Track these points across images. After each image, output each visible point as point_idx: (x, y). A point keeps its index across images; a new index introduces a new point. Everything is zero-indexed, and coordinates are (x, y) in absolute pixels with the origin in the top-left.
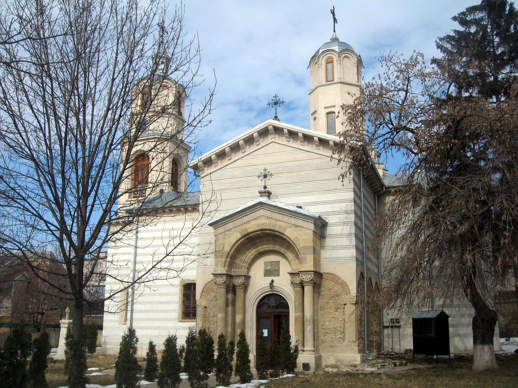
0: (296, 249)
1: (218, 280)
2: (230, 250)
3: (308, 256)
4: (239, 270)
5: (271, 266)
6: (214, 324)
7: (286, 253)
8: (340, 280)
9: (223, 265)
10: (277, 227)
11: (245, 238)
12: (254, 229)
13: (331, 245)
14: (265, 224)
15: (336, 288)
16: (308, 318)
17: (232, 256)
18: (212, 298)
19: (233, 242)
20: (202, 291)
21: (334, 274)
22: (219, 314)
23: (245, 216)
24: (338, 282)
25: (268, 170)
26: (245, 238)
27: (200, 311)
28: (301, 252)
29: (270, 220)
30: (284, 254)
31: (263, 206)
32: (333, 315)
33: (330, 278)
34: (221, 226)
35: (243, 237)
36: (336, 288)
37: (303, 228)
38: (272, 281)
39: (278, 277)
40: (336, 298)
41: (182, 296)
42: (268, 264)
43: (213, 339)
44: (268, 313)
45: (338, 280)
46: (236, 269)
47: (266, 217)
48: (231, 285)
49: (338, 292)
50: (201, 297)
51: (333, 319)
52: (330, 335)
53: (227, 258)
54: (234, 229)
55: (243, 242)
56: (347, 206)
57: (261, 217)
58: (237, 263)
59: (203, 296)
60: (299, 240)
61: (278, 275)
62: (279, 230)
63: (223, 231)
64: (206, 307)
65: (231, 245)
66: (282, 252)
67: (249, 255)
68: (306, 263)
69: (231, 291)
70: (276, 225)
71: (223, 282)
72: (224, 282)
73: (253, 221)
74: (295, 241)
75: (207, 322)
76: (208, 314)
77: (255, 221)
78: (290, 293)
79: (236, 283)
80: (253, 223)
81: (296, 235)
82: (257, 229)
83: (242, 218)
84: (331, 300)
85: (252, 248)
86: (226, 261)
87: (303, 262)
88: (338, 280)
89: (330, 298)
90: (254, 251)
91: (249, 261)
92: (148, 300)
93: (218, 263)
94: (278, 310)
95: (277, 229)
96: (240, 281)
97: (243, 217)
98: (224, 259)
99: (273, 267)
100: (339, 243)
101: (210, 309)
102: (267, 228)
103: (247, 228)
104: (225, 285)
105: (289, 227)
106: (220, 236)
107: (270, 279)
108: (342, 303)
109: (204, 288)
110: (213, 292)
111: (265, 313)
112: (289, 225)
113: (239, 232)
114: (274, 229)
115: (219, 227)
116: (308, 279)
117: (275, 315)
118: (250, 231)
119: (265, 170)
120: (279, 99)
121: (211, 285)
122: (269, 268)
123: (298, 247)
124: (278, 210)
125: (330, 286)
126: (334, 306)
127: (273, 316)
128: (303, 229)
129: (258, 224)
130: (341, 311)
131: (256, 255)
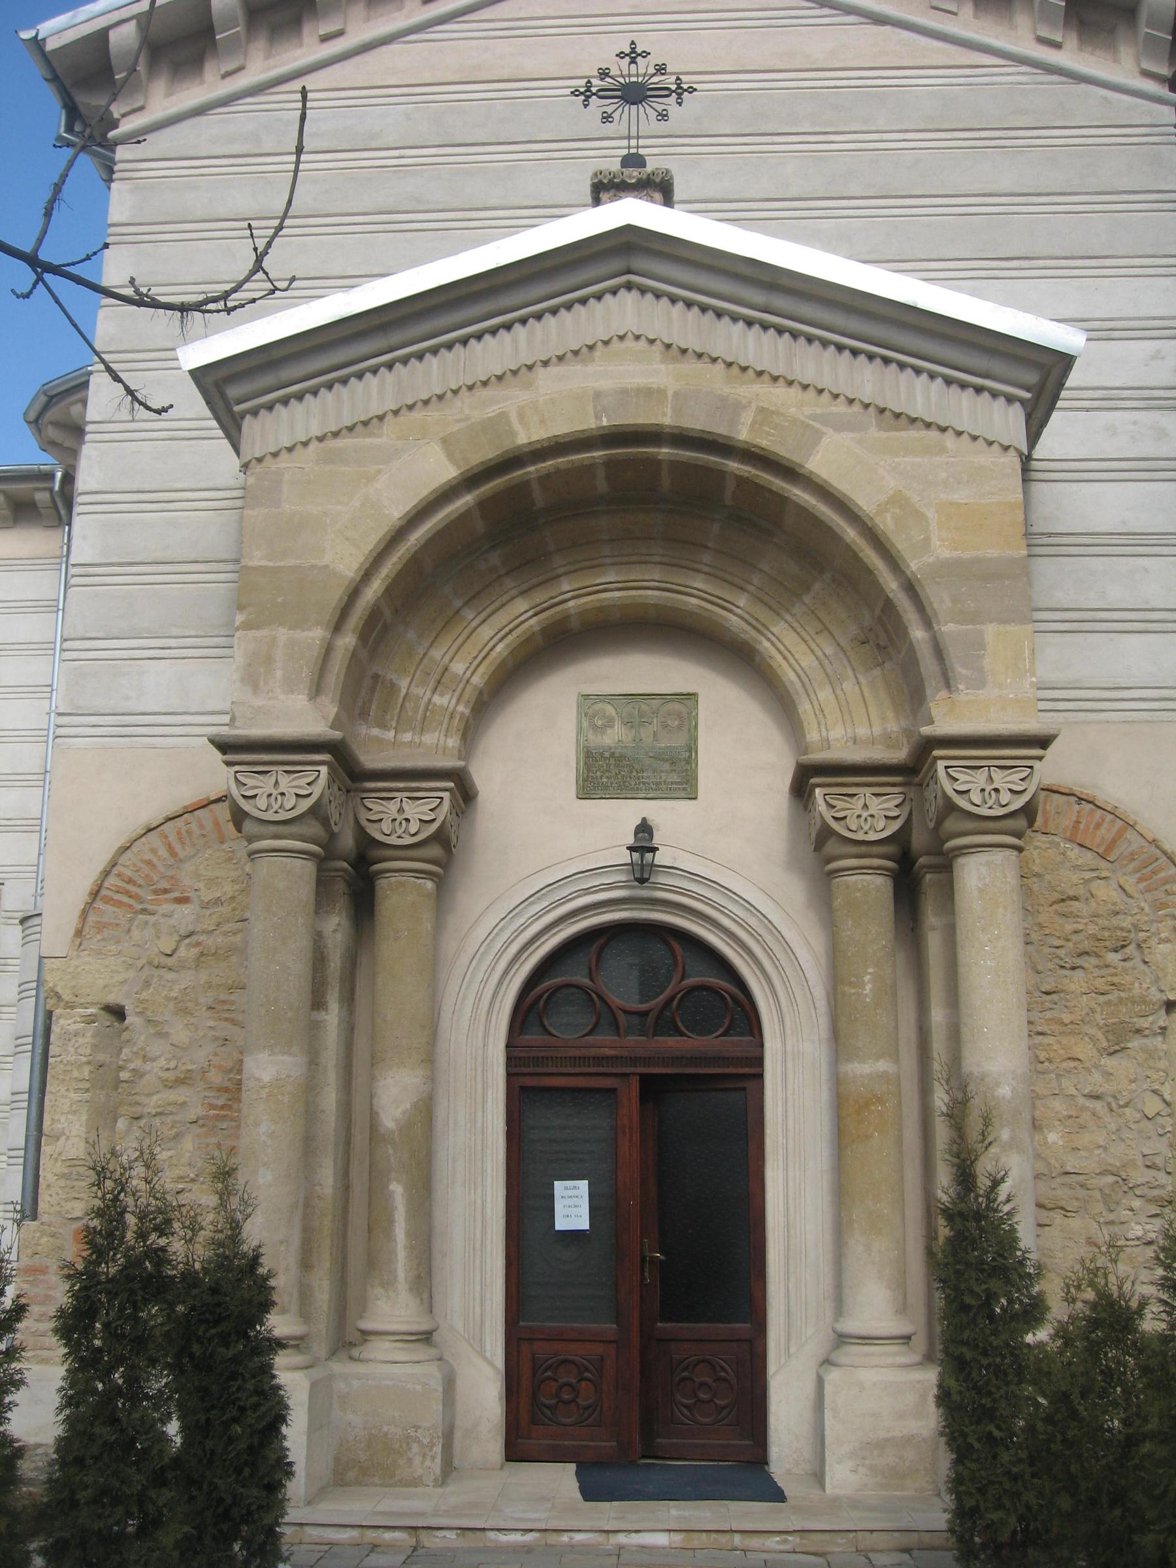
0: (891, 585)
1: (262, 785)
2: (367, 576)
3: (990, 631)
4: (407, 737)
5: (628, 723)
7: (760, 628)
8: (1130, 835)
9: (306, 674)
10: (747, 418)
11: (487, 488)
12: (562, 426)
13: (1061, 597)
14: (648, 393)
15: (1106, 892)
16: (1004, 1091)
17: (374, 616)
18: (167, 944)
19: (396, 510)
20: (95, 894)
21: (1086, 792)
22: (264, 1056)
23: (494, 331)
24: (1121, 849)
25: (653, 60)
26: (487, 488)
27: (67, 1036)
28: (939, 599)
29: (690, 366)
30: (748, 633)
31: (640, 263)
32: (1097, 1077)
33: (1067, 822)
34: (300, 397)
35: (470, 481)
36: (1106, 892)
37: (949, 435)
38: (644, 829)
39: (684, 806)
40: (1113, 958)
42: (610, 710)
43: (262, 1271)
44: (599, 1060)
45: (1120, 834)
46: (384, 726)
47: (658, 347)
48: (347, 841)
49: (1126, 922)
50: (79, 933)
51: (1098, 1105)
52: (1075, 1223)
53: (338, 627)
54: (406, 417)
55: (462, 519)
56: (1157, 356)
57: (616, 345)
58: (393, 687)
59: (101, 927)
60: (920, 516)
61: (687, 788)
62: (765, 441)
63: (316, 431)
64: (118, 1013)
65: (372, 539)
66: (734, 622)
67: (486, 632)
68: (980, 682)
69: (340, 887)
70: (738, 407)
71: (305, 805)
72: (316, 812)
73: (552, 370)
74: (886, 523)
75: (121, 1124)
76: (137, 1064)
77: (573, 369)
78: (775, 917)
79: (386, 827)
80: (548, 382)
81: (892, 483)
82: (589, 422)
83: (464, 341)
84: (1079, 972)
85: (509, 583)
86: (328, 650)
87: (960, 670)
88: (1120, 834)
89: (1070, 961)
90: (521, 605)
91: (478, 680)
93: (269, 660)
94: (671, 1043)
95: (743, 434)
96: (417, 811)
97: (479, 337)
98: (316, 634)
99: (646, 733)
100: (1117, 595)
102: (666, 418)
103: (503, 415)
104: (314, 828)
105: (840, 425)
106: (284, 461)
107: (628, 813)
108: (1155, 996)
109: (106, 873)
111: (574, 1061)
112: (840, 407)
113: (445, 442)
114: (719, 428)
115: (285, 401)
116: (1005, 797)
117: (645, 1080)
118: (526, 435)
119: (633, 55)
121: (163, 852)
122: (615, 736)
123: (914, 565)
124: (758, 297)
125: (1068, 880)
126: (1099, 1018)
127: (635, 1083)
128: (949, 440)
129: (598, 395)
130: (1151, 1054)
131: (528, 640)
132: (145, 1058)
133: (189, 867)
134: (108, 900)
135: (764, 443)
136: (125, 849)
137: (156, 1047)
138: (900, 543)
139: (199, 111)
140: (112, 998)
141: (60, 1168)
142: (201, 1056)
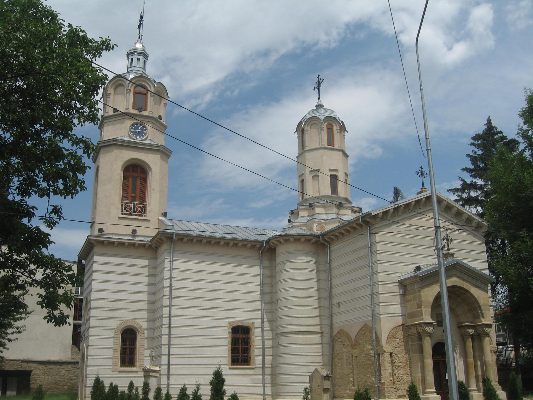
6: (400, 369)
14: (456, 281)
27: (387, 357)
28: (483, 308)
41: (230, 340)
59: (389, 342)
74: (478, 299)
92: (188, 343)
101: (396, 355)
110: (397, 339)
120: (419, 170)
123: (481, 304)
129: (452, 281)
132: (396, 359)
133: (397, 334)
134: (389, 339)
135: (467, 289)
136: (390, 332)
137: (397, 358)
138: (479, 301)
139: (385, 225)
140: (391, 351)
141: (389, 374)
142: (401, 359)
